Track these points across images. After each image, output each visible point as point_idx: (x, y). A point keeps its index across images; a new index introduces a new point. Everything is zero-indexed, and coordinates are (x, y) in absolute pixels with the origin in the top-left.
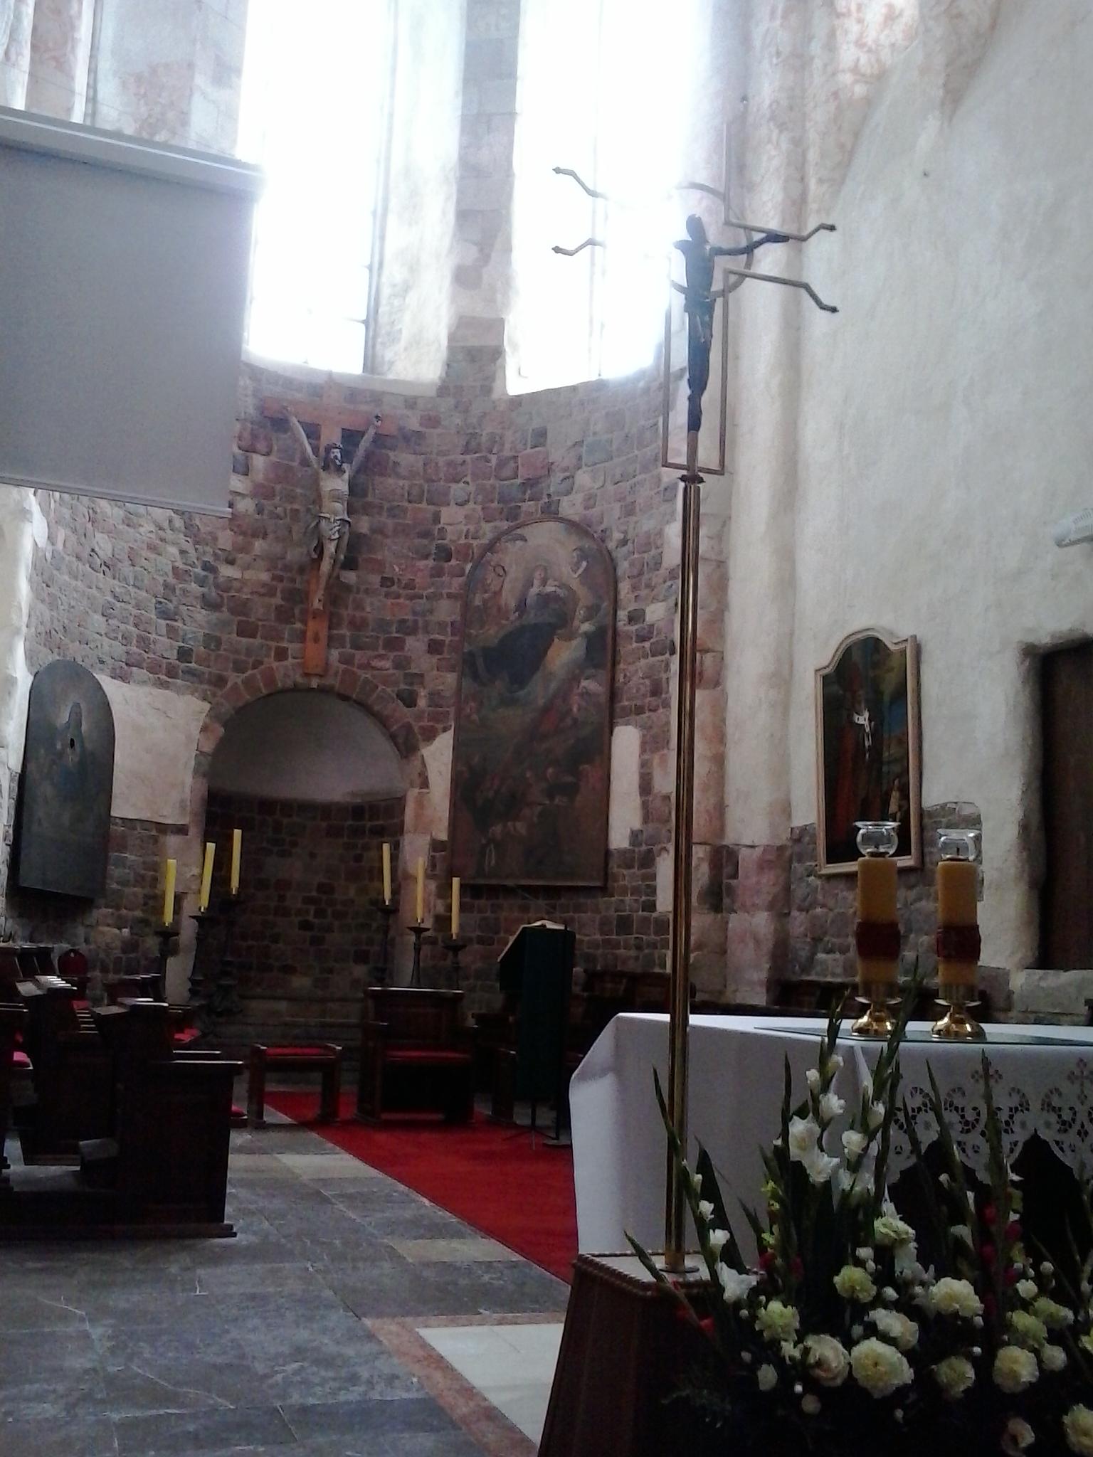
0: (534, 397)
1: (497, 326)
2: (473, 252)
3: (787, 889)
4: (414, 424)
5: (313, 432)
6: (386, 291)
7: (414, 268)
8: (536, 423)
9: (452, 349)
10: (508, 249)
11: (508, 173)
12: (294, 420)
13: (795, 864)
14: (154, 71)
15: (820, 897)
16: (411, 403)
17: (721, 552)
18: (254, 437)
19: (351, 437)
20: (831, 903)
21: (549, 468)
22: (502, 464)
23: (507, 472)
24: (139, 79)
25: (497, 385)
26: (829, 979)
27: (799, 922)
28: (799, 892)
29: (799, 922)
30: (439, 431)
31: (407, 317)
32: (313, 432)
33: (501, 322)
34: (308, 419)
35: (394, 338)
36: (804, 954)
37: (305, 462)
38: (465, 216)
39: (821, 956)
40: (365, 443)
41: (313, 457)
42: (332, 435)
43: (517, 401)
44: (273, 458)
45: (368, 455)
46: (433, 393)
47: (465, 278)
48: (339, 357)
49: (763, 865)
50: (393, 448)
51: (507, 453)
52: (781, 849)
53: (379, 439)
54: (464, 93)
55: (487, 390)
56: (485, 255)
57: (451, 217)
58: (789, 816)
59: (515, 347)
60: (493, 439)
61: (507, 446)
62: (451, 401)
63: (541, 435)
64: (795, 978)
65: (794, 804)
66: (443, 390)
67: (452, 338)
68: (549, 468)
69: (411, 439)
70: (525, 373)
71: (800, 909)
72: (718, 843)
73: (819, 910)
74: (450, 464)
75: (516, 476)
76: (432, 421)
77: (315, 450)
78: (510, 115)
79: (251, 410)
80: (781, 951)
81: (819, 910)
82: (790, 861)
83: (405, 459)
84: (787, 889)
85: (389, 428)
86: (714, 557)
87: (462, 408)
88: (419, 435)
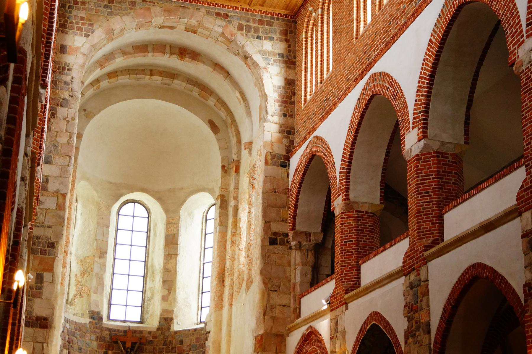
0: (180, 332)
1: (171, 312)
2: (166, 292)
4: (151, 338)
5: (124, 343)
6: (146, 299)
7: (153, 294)
8: (181, 338)
9: (160, 318)
10: (175, 291)
11: (176, 271)
12: (119, 342)
14: (85, 258)
16: (150, 333)
18: (109, 346)
19: (134, 344)
21: (183, 351)
22: (172, 348)
23: (173, 351)
24: (81, 261)
25: (171, 328)
30: (157, 340)
31: (151, 307)
32: (124, 343)
33: (173, 311)
34: (122, 341)
35: (148, 312)
37: (122, 351)
38: (164, 282)
40: (137, 346)
41: (124, 351)
42: (129, 345)
43: (176, 332)
44: (114, 351)
45: (138, 347)
46: (156, 330)
47: (164, 299)
48: (134, 315)
50: (145, 345)
51: (174, 346)
53: (140, 344)
54: (165, 248)
55: (169, 329)
56: (169, 293)
57: (161, 282)
59: (176, 317)
60: (170, 341)
61: (174, 344)
62: (160, 332)
63: (181, 342)
66: (158, 329)
67: (161, 315)
68: (183, 351)
69: (151, 342)
70: (176, 327)
74: (159, 348)
75: (175, 352)
76: (155, 337)
77: (124, 349)
78: (177, 255)
79: (109, 340)
83: (148, 348)
85: (144, 341)
87: (163, 333)
88: (151, 341)
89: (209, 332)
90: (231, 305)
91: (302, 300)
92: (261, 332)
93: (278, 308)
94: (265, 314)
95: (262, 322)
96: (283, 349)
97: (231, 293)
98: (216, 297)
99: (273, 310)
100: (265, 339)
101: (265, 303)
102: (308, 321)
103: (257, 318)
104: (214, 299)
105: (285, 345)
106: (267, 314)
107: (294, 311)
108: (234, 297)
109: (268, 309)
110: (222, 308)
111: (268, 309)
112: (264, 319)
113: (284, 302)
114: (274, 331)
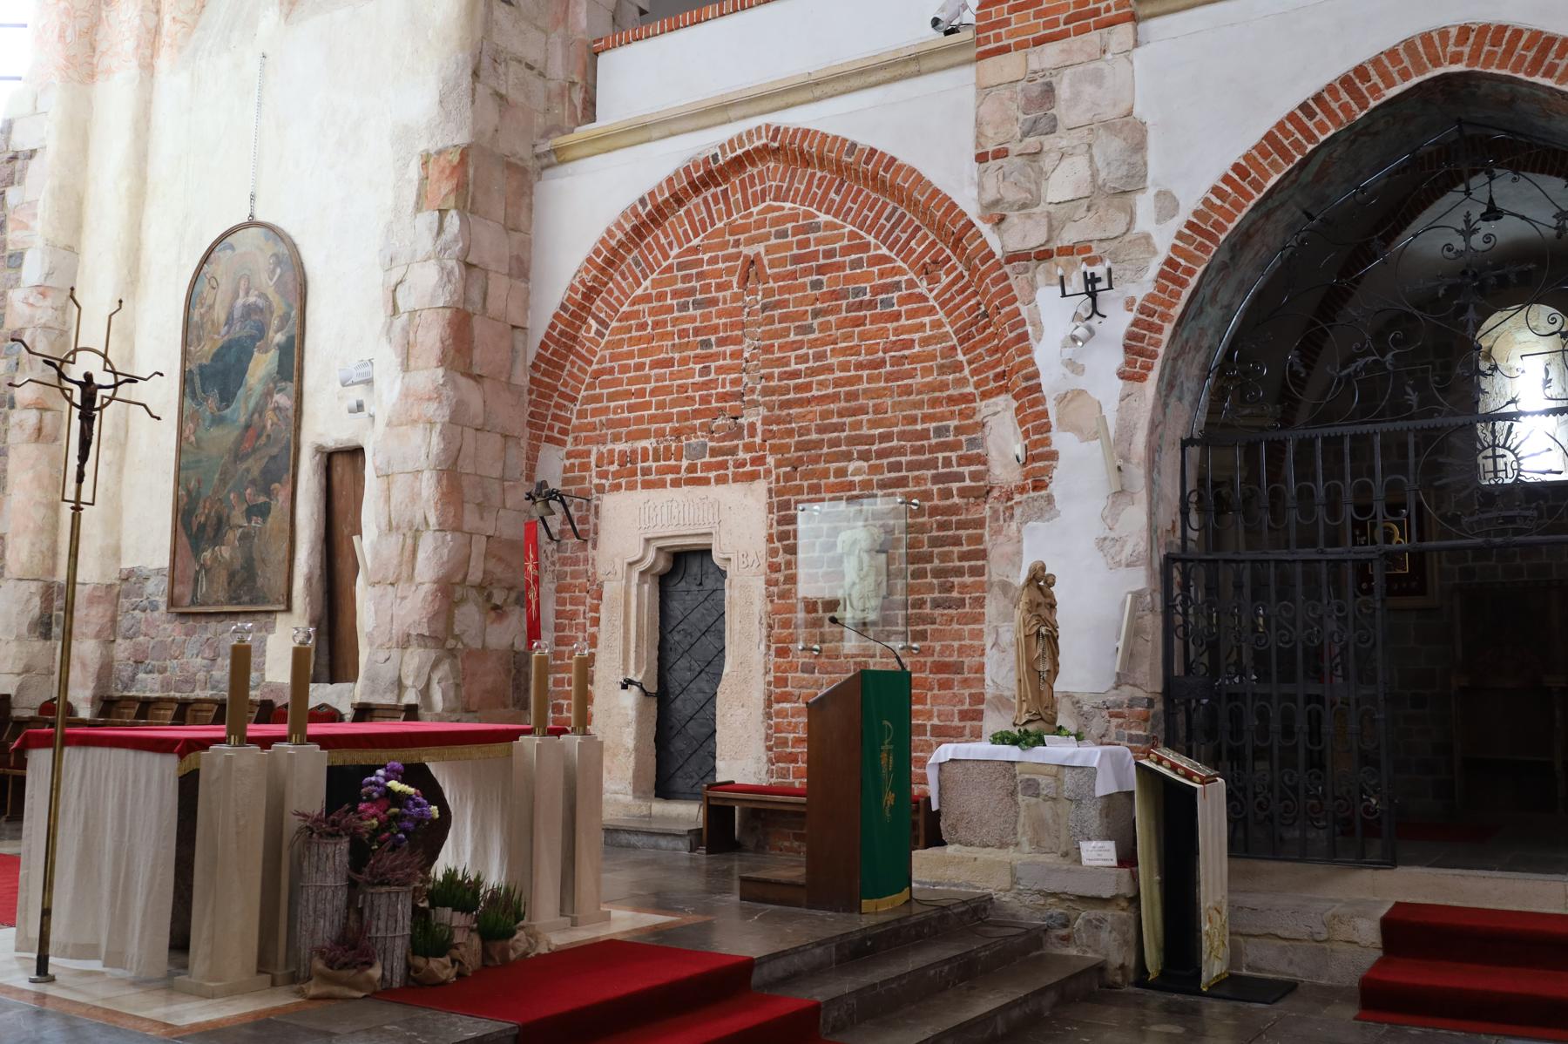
3: (114, 621)
13: (122, 600)
15: (143, 628)
17: (64, 323)
20: (153, 632)
26: (148, 694)
27: (122, 650)
28: (125, 623)
29: (122, 650)
36: (126, 674)
39: (141, 676)
49: (92, 601)
52: (110, 586)
58: (119, 560)
64: (117, 694)
65: (123, 550)
71: (125, 638)
72: (50, 579)
73: (141, 638)
80: (106, 671)
81: (141, 638)
82: (118, 595)
84: (114, 621)
86: (56, 325)
89: (32, 154)
90: (148, 68)
91: (602, 58)
92: (462, 138)
93: (514, 66)
94: (475, 74)
95: (467, 100)
96: (523, 218)
97: (152, 25)
98: (69, 32)
99: (501, 69)
100: (476, 169)
101: (479, 34)
102: (732, 113)
103: (445, 81)
104: (62, 36)
105: (530, 208)
106: (482, 74)
107: (562, 95)
108: (165, 39)
109: (486, 62)
110: (92, 76)
111: (486, 62)
112: (474, 90)
113: (533, 54)
114: (504, 147)
